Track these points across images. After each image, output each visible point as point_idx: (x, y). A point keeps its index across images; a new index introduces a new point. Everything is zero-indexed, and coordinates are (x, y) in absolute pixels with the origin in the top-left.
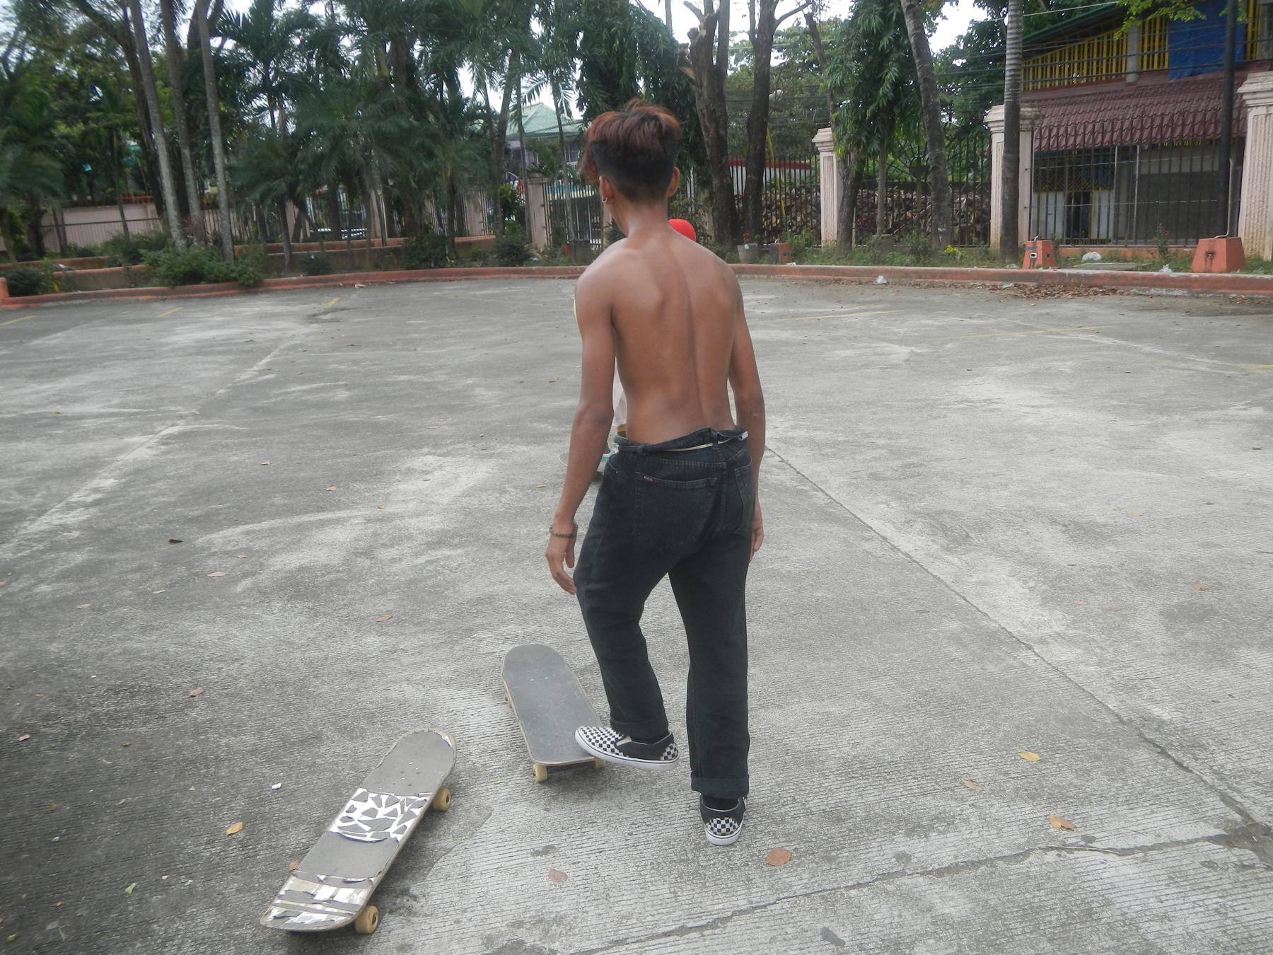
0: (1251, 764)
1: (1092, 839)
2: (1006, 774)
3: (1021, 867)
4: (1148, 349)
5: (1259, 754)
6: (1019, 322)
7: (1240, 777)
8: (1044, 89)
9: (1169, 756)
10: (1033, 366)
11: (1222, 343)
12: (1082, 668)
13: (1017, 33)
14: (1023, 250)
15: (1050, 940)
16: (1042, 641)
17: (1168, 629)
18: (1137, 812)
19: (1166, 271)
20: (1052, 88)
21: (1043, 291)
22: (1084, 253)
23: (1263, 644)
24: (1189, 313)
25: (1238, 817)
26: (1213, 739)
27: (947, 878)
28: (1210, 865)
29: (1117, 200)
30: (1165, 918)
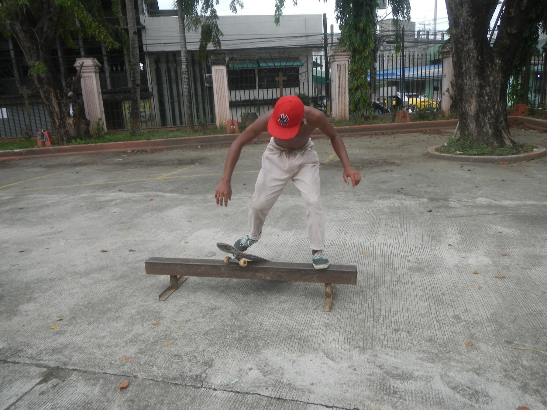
0: (42, 347)
5: (43, 342)
7: (40, 354)
9: (8, 362)
18: (4, 391)
23: (28, 301)
25: (45, 369)
26: (24, 346)
28: (43, 393)
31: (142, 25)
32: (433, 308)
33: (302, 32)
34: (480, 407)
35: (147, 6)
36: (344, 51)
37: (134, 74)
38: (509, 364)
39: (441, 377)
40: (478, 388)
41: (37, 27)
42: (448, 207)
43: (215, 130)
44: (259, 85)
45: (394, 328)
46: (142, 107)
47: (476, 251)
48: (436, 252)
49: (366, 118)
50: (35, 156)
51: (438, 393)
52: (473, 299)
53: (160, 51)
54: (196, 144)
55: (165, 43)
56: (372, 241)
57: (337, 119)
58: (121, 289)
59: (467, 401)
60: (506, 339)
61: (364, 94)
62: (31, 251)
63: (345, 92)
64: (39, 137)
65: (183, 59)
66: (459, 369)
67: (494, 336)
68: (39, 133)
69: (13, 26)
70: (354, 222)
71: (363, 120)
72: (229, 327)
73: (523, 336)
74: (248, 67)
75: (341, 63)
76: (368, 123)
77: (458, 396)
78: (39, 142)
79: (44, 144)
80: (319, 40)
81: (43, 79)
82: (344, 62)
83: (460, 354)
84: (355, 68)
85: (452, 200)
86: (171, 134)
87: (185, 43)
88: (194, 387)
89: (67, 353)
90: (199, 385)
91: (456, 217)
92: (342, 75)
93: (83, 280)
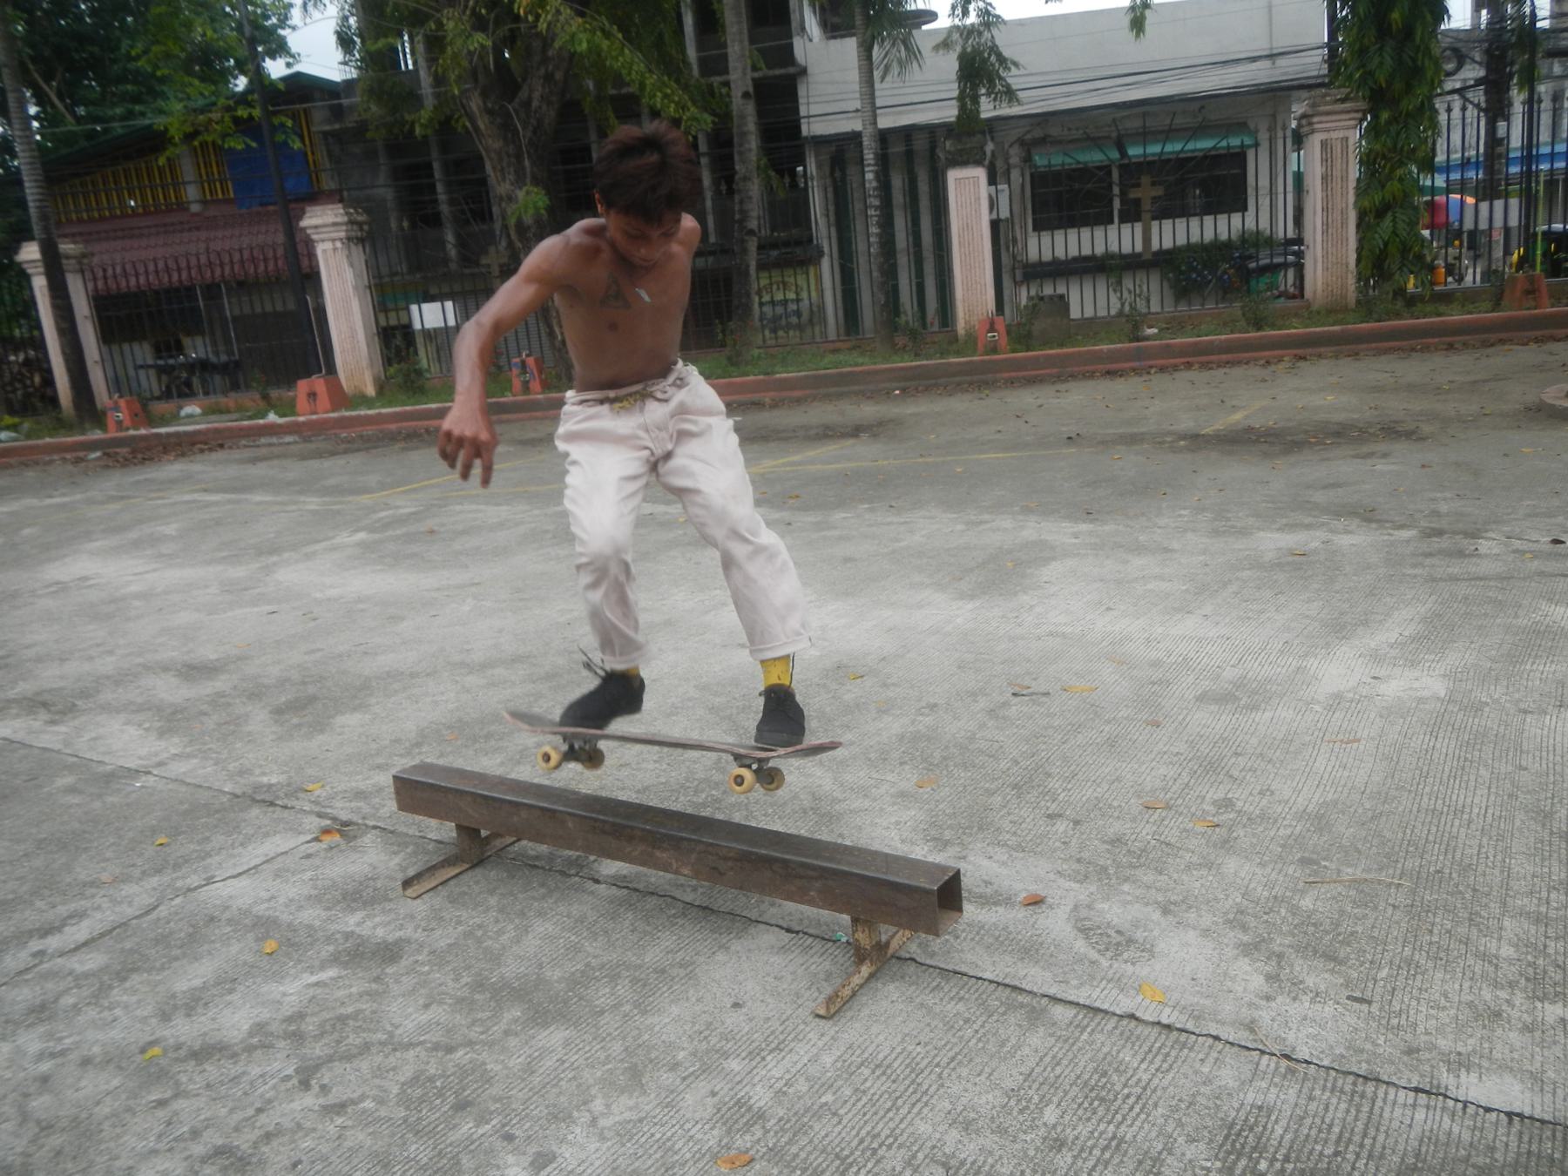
1: (213, 877)
2: (133, 866)
3: (154, 915)
4: (257, 498)
6: (114, 493)
8: (91, 220)
10: (133, 535)
11: (332, 481)
12: (200, 772)
13: (31, 157)
14: (104, 413)
15: (181, 947)
16: (160, 764)
17: (276, 722)
18: (250, 848)
19: (272, 417)
20: (102, 219)
21: (140, 456)
22: (181, 408)
23: (355, 709)
24: (303, 457)
25: (328, 822)
27: (84, 949)
28: (308, 856)
29: (214, 344)
30: (273, 897)
31: (799, 66)
32: (1185, 777)
33: (1260, 45)
34: (1111, 966)
35: (823, 9)
36: (1343, 101)
37: (741, 202)
38: (1263, 900)
39: (1076, 907)
40: (1139, 935)
41: (517, 100)
42: (1461, 554)
43: (952, 343)
44: (1120, 211)
45: (1050, 812)
46: (794, 288)
47: (1427, 665)
48: (1312, 664)
49: (1411, 301)
50: (505, 417)
51: (1040, 935)
52: (1308, 769)
53: (847, 133)
54: (887, 385)
55: (857, 111)
56: (1160, 630)
57: (1315, 307)
58: (532, 699)
59: (1094, 955)
60: (1306, 855)
61: (1401, 225)
62: (402, 619)
63: (1344, 224)
64: (516, 371)
65: (869, 157)
66: (1129, 898)
67: (1283, 846)
68: (517, 360)
69: (464, 101)
70: (1149, 586)
71: (1400, 304)
72: (696, 783)
73: (1359, 852)
74: (1050, 166)
75: (1334, 135)
76: (1412, 317)
77: (1080, 945)
78: (517, 383)
79: (526, 384)
80: (1314, 64)
81: (529, 227)
82: (1341, 134)
83: (1161, 874)
84: (1378, 147)
85: (1494, 536)
86: (830, 358)
87: (874, 108)
88: (563, 873)
89: (377, 800)
90: (573, 872)
91: (1458, 580)
92: (1337, 173)
93: (471, 680)
